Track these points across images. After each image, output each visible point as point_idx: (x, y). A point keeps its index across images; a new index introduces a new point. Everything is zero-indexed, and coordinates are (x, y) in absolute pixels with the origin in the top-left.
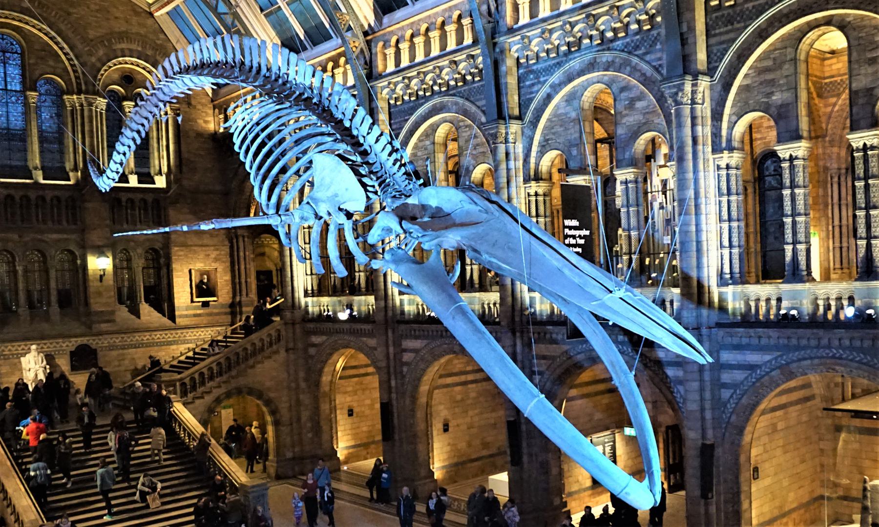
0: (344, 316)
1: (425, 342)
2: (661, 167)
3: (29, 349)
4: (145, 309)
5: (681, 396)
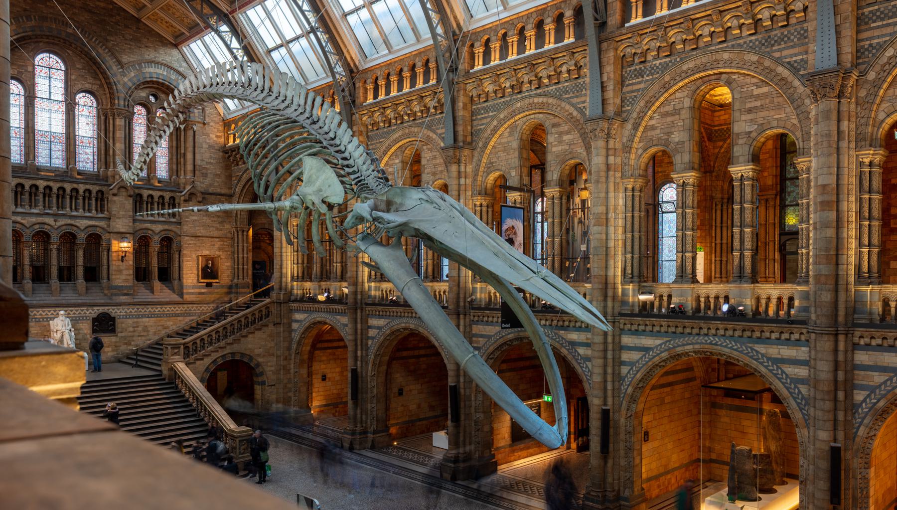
0: (322, 298)
1: (387, 321)
2: (582, 189)
3: (58, 314)
4: (157, 284)
5: (589, 370)
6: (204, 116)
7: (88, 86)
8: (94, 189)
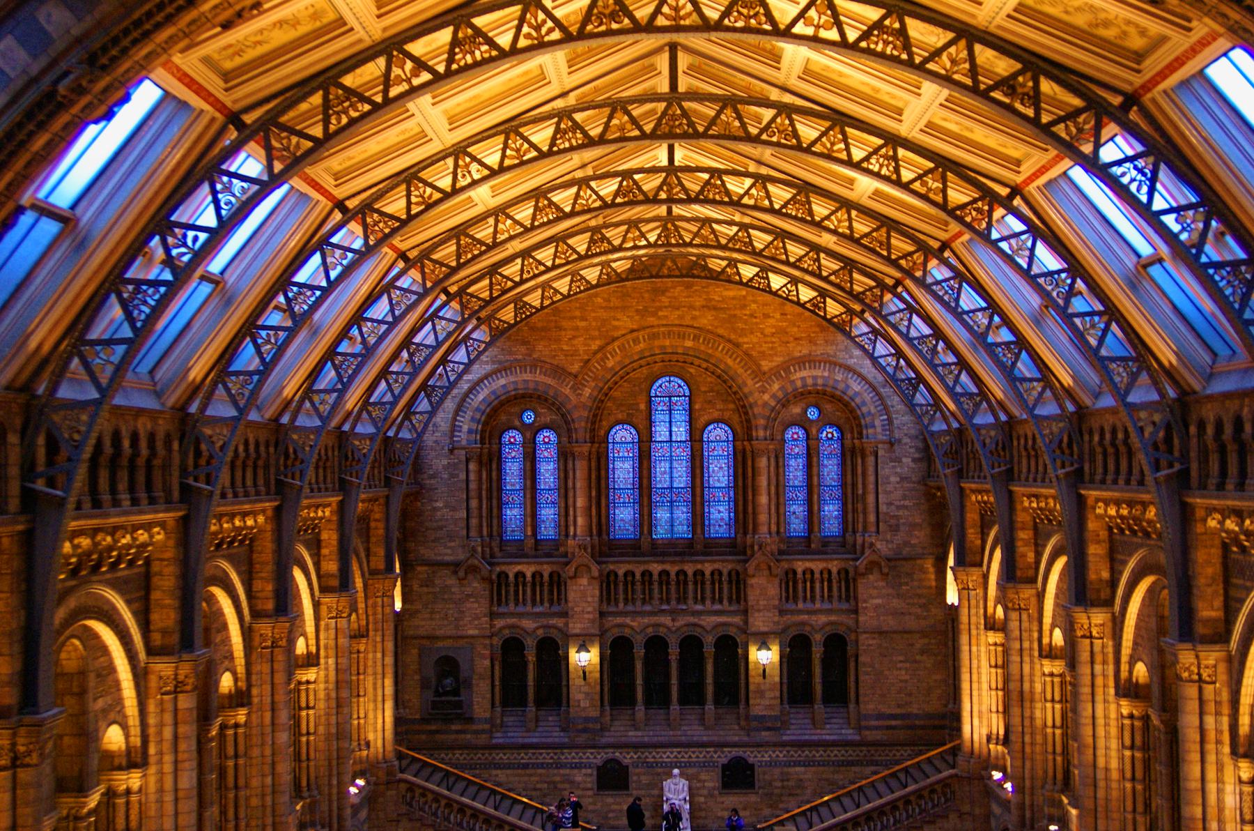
6: (891, 431)
7: (716, 414)
8: (726, 568)
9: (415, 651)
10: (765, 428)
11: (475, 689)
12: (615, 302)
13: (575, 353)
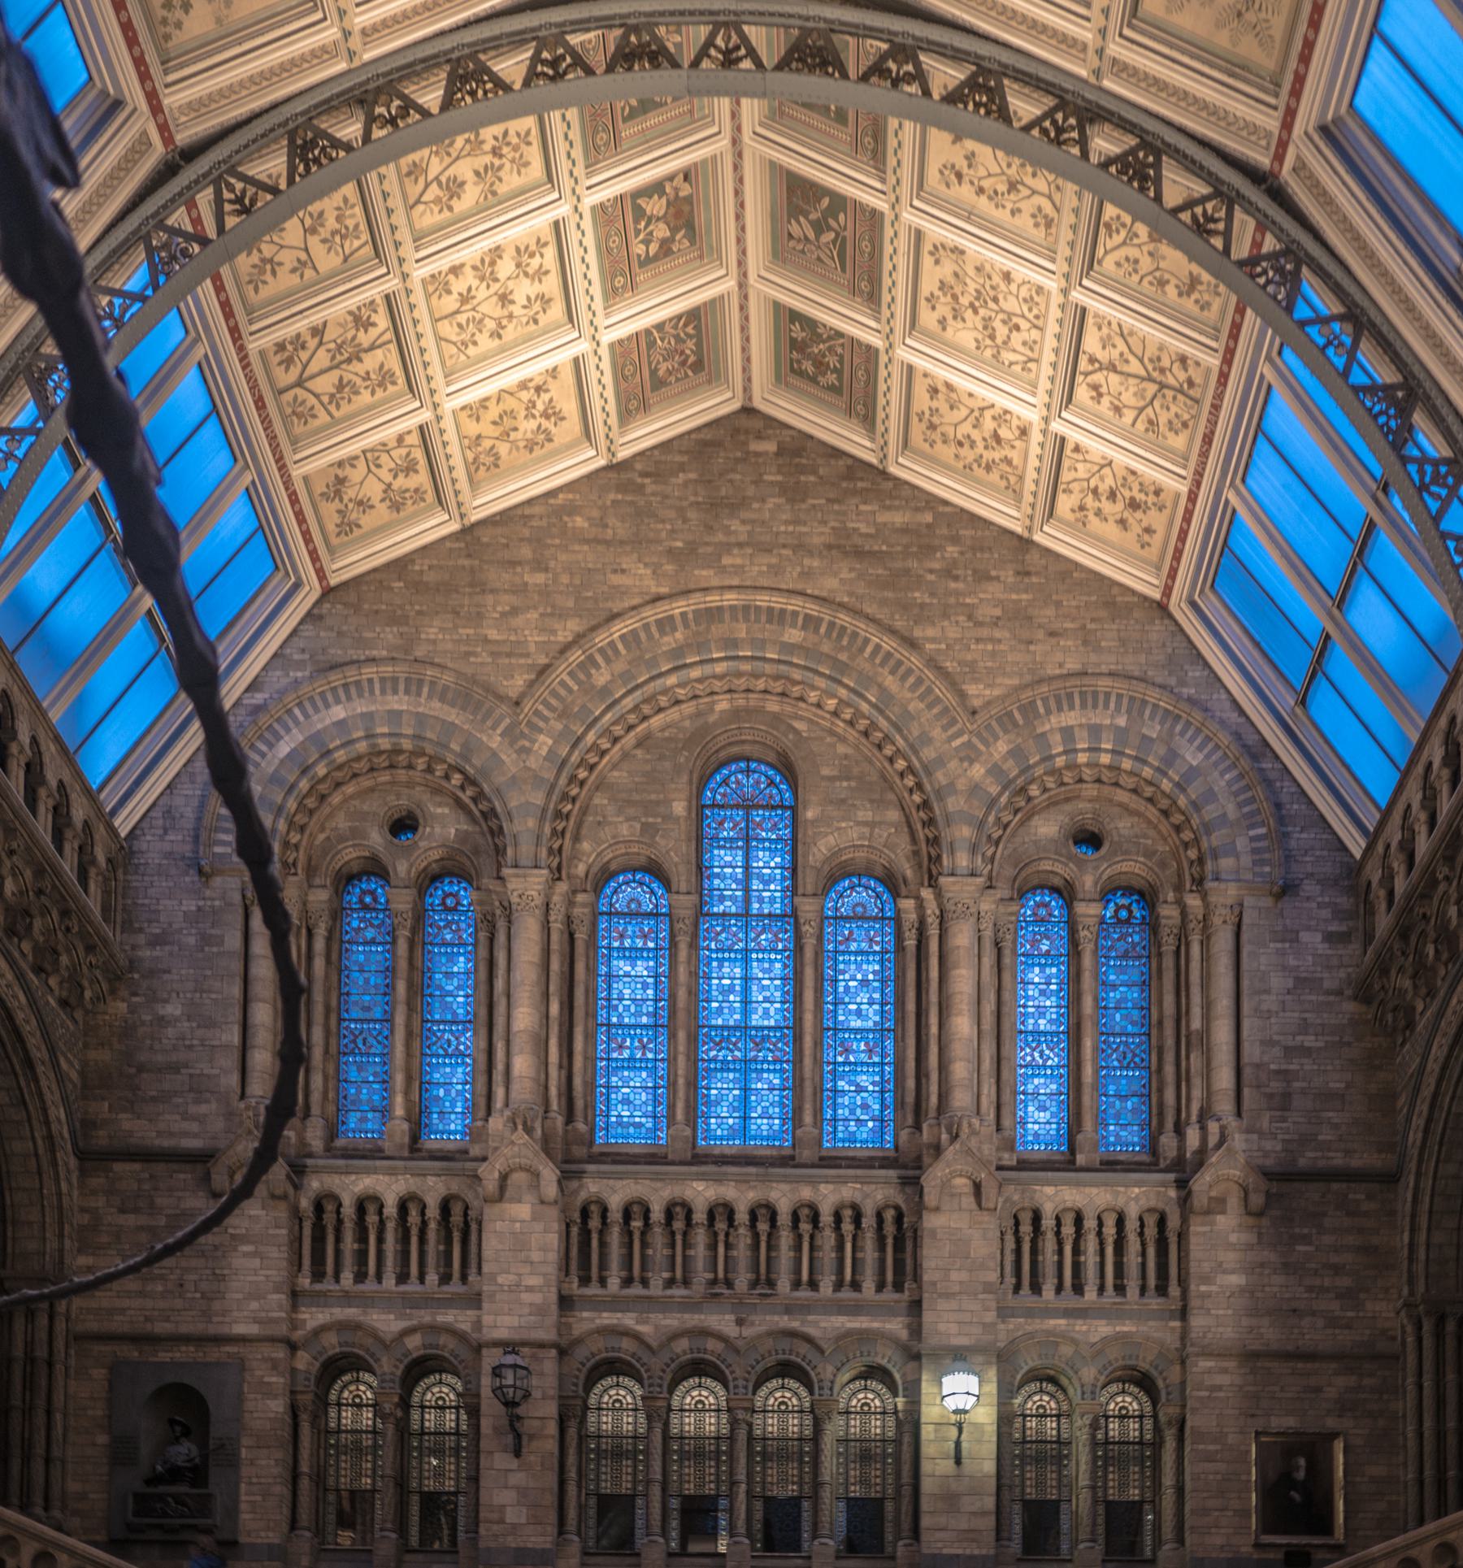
9: (99, 1373)
10: (974, 849)
11: (245, 1471)
12: (618, 528)
13: (516, 650)
